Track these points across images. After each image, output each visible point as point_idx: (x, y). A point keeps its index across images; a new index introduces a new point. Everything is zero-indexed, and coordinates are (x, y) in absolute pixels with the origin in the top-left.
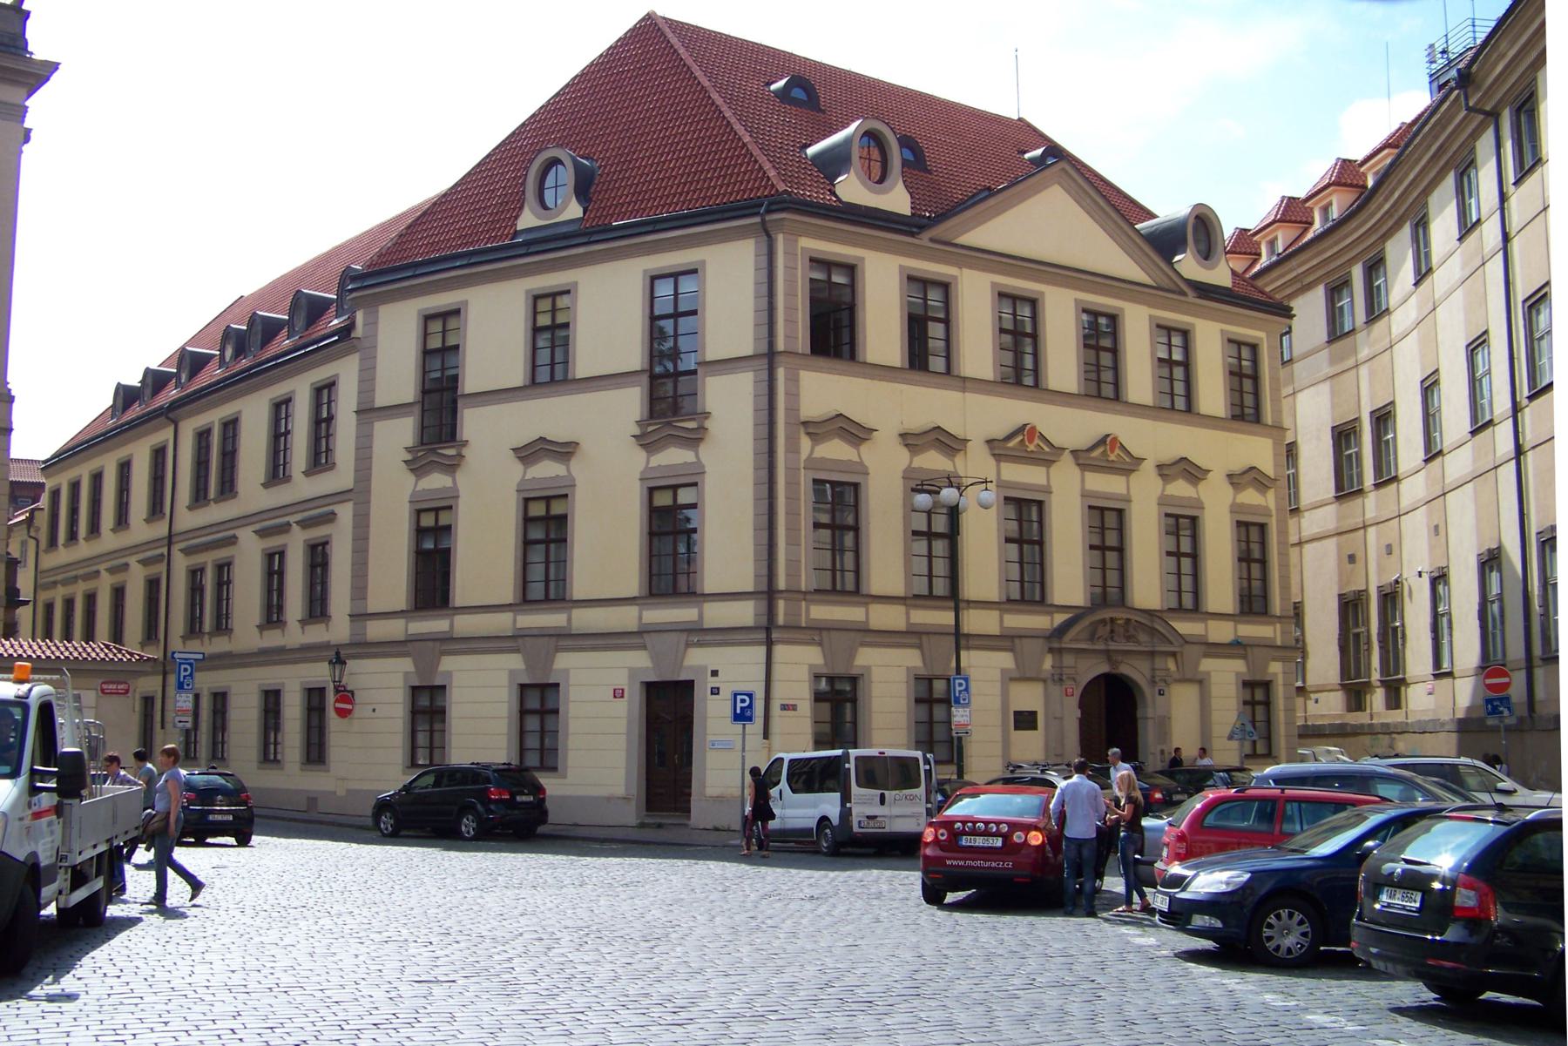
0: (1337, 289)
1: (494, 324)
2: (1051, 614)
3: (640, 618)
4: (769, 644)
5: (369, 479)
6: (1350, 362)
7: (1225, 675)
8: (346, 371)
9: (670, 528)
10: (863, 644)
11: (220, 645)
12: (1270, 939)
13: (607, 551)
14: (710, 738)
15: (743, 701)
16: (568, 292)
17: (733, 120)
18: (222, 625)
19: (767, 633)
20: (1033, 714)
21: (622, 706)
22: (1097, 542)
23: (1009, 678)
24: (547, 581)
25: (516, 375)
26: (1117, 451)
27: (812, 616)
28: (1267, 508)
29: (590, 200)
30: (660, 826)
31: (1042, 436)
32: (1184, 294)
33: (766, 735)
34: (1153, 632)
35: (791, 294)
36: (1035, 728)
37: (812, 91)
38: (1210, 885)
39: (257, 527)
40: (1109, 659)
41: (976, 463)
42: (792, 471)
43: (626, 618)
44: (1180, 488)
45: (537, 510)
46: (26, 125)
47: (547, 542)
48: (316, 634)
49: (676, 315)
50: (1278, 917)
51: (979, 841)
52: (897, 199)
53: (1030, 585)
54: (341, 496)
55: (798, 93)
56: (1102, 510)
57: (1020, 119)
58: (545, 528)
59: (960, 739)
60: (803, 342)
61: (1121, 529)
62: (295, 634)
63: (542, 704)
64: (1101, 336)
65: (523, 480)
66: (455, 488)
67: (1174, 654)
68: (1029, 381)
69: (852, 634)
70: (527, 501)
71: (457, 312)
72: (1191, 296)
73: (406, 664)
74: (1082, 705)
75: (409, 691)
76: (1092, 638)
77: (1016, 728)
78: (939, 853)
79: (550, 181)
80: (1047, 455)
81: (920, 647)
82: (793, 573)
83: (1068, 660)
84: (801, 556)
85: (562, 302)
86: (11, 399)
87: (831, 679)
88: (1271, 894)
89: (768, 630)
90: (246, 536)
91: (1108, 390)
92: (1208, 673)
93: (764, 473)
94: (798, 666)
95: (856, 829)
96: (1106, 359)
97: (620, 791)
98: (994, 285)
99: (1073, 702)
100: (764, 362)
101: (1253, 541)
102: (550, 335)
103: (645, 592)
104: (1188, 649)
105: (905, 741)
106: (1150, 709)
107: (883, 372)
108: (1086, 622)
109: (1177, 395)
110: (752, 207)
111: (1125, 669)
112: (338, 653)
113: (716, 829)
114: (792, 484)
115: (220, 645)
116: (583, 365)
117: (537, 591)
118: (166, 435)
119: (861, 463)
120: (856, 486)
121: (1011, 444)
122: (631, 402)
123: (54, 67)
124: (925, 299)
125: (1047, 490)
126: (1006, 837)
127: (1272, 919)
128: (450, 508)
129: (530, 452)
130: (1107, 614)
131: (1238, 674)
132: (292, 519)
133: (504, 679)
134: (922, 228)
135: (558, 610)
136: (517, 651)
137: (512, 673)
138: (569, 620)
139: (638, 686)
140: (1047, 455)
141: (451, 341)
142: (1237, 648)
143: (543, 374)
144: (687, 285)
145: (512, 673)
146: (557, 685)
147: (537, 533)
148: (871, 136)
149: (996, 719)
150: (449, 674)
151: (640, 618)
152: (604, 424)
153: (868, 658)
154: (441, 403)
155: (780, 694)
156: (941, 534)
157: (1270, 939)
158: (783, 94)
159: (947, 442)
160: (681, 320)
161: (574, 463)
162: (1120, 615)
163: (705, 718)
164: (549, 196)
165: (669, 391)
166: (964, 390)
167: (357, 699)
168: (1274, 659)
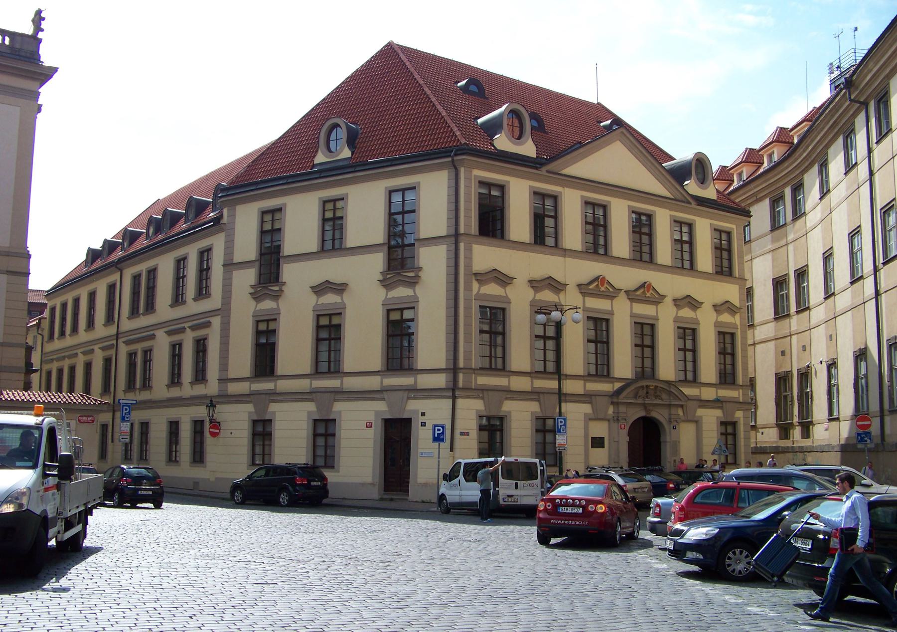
0: (776, 201)
1: (301, 217)
2: (613, 382)
4: (454, 398)
6: (783, 242)
7: (711, 418)
8: (218, 242)
9: (399, 332)
10: (506, 399)
11: (145, 396)
12: (729, 565)
13: (363, 345)
14: (420, 451)
15: (439, 430)
16: (343, 199)
17: (436, 103)
18: (147, 385)
19: (453, 392)
21: (371, 431)
22: (639, 342)
23: (589, 419)
24: (329, 361)
25: (313, 245)
26: (651, 291)
27: (479, 382)
28: (735, 324)
29: (356, 147)
30: (392, 500)
32: (689, 203)
33: (452, 449)
34: (670, 393)
35: (468, 201)
37: (482, 87)
38: (697, 535)
39: (166, 329)
40: (645, 408)
41: (571, 297)
42: (468, 301)
43: (373, 383)
44: (686, 313)
45: (324, 321)
46: (39, 102)
47: (329, 339)
48: (200, 390)
49: (403, 213)
50: (734, 553)
51: (569, 510)
52: (528, 149)
53: (601, 366)
54: (214, 312)
55: (473, 88)
56: (642, 324)
57: (598, 103)
58: (329, 332)
59: (561, 452)
60: (474, 228)
61: (653, 335)
62: (187, 390)
63: (326, 431)
64: (642, 227)
65: (317, 305)
66: (278, 309)
67: (682, 406)
68: (601, 251)
70: (318, 316)
71: (280, 210)
72: (693, 204)
75: (251, 424)
76: (636, 396)
77: (592, 447)
78: (547, 516)
79: (333, 136)
80: (611, 293)
81: (538, 400)
82: (467, 359)
83: (622, 409)
84: (472, 349)
85: (339, 204)
86: (29, 256)
87: (489, 418)
88: (730, 541)
89: (453, 390)
90: (161, 334)
91: (646, 257)
92: (701, 417)
93: (452, 302)
94: (470, 411)
95: (501, 502)
96: (645, 239)
97: (369, 480)
98: (582, 197)
99: (625, 432)
100: (453, 239)
101: (727, 343)
102: (332, 223)
103: (385, 368)
104: (690, 403)
105: (529, 453)
106: (668, 436)
107: (519, 245)
108: (633, 387)
109: (685, 261)
110: (446, 152)
111: (654, 414)
112: (211, 401)
113: (423, 502)
114: (468, 308)
115: (145, 396)
116: (351, 240)
117: (324, 367)
118: (115, 277)
119: (507, 297)
120: (504, 310)
121: (591, 287)
122: (377, 262)
123: (55, 70)
124: (544, 205)
125: (611, 313)
126: (585, 508)
127: (731, 554)
129: (320, 289)
130: (644, 383)
132: (186, 325)
133: (304, 416)
134: (542, 165)
135: (335, 378)
136: (312, 400)
137: (309, 413)
138: (342, 383)
140: (611, 293)
141: (277, 226)
142: (718, 403)
143: (329, 245)
144: (409, 196)
145: (309, 413)
146: (335, 420)
147: (324, 334)
148: (514, 113)
149: (581, 442)
150: (274, 413)
152: (363, 274)
154: (270, 261)
155: (460, 426)
156: (551, 337)
157: (729, 565)
158: (465, 89)
159: (555, 285)
160: (406, 215)
161: (345, 295)
163: (417, 439)
164: (332, 145)
165: (399, 256)
166: (565, 256)
168: (738, 410)
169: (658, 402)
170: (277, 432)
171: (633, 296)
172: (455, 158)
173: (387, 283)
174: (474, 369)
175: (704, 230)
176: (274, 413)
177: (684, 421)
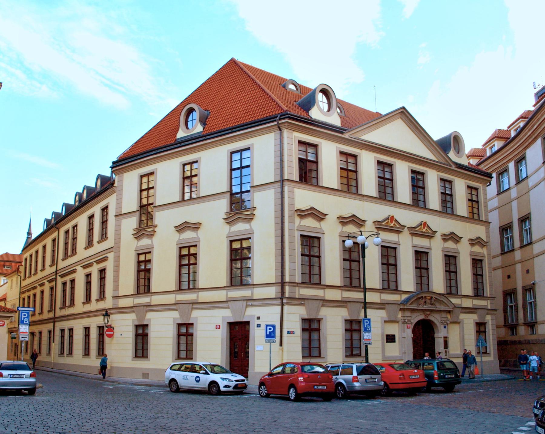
2: (400, 294)
3: (227, 295)
4: (282, 305)
5: (119, 243)
7: (469, 321)
10: (322, 306)
13: (213, 267)
15: (270, 329)
19: (282, 300)
20: (394, 336)
24: (189, 281)
31: (396, 221)
33: (281, 344)
36: (394, 342)
43: (221, 295)
44: (450, 245)
45: (185, 252)
47: (189, 265)
48: (102, 305)
49: (241, 168)
54: (110, 250)
58: (187, 258)
59: (366, 346)
60: (296, 177)
62: (94, 306)
65: (179, 240)
67: (449, 312)
69: (318, 301)
73: (133, 316)
74: (414, 332)
77: (387, 342)
80: (397, 229)
82: (292, 275)
83: (408, 314)
84: (295, 269)
89: (281, 299)
90: (79, 268)
92: (463, 320)
93: (279, 220)
94: (294, 316)
98: (375, 157)
100: (279, 184)
103: (229, 284)
106: (439, 335)
111: (431, 318)
112: (107, 312)
114: (291, 236)
117: (185, 285)
119: (321, 228)
122: (224, 204)
128: (150, 252)
129: (182, 228)
131: (474, 320)
133: (171, 322)
136: (176, 310)
137: (174, 319)
139: (226, 324)
140: (397, 229)
145: (174, 319)
146: (192, 324)
149: (380, 339)
150: (150, 320)
151: (227, 295)
152: (212, 215)
153: (325, 313)
162: (429, 296)
167: (115, 330)
168: (488, 314)
169: (433, 308)
170: (151, 333)
171: (415, 232)
172: (280, 122)
173: (230, 220)
174: (297, 283)
175: (460, 187)
176: (150, 320)
177: (451, 323)
